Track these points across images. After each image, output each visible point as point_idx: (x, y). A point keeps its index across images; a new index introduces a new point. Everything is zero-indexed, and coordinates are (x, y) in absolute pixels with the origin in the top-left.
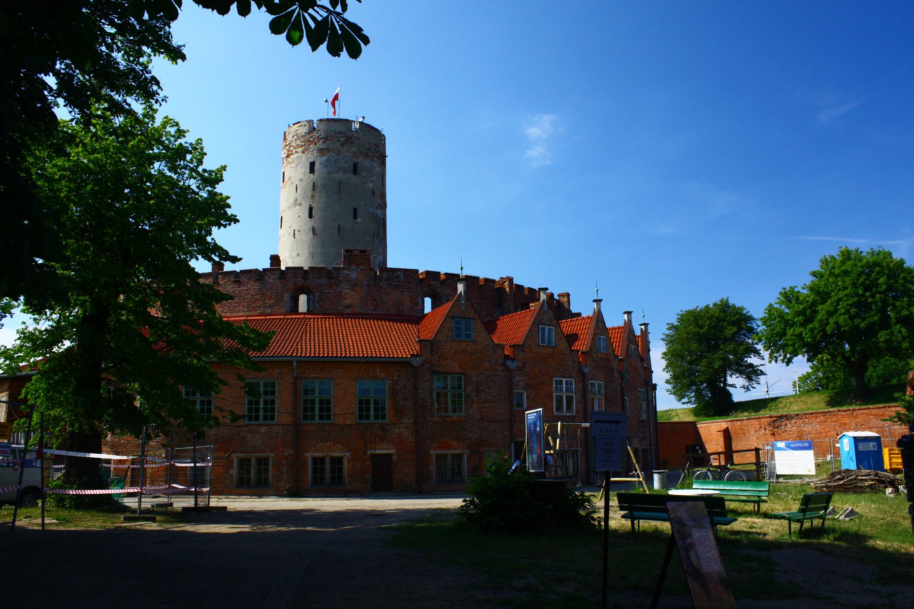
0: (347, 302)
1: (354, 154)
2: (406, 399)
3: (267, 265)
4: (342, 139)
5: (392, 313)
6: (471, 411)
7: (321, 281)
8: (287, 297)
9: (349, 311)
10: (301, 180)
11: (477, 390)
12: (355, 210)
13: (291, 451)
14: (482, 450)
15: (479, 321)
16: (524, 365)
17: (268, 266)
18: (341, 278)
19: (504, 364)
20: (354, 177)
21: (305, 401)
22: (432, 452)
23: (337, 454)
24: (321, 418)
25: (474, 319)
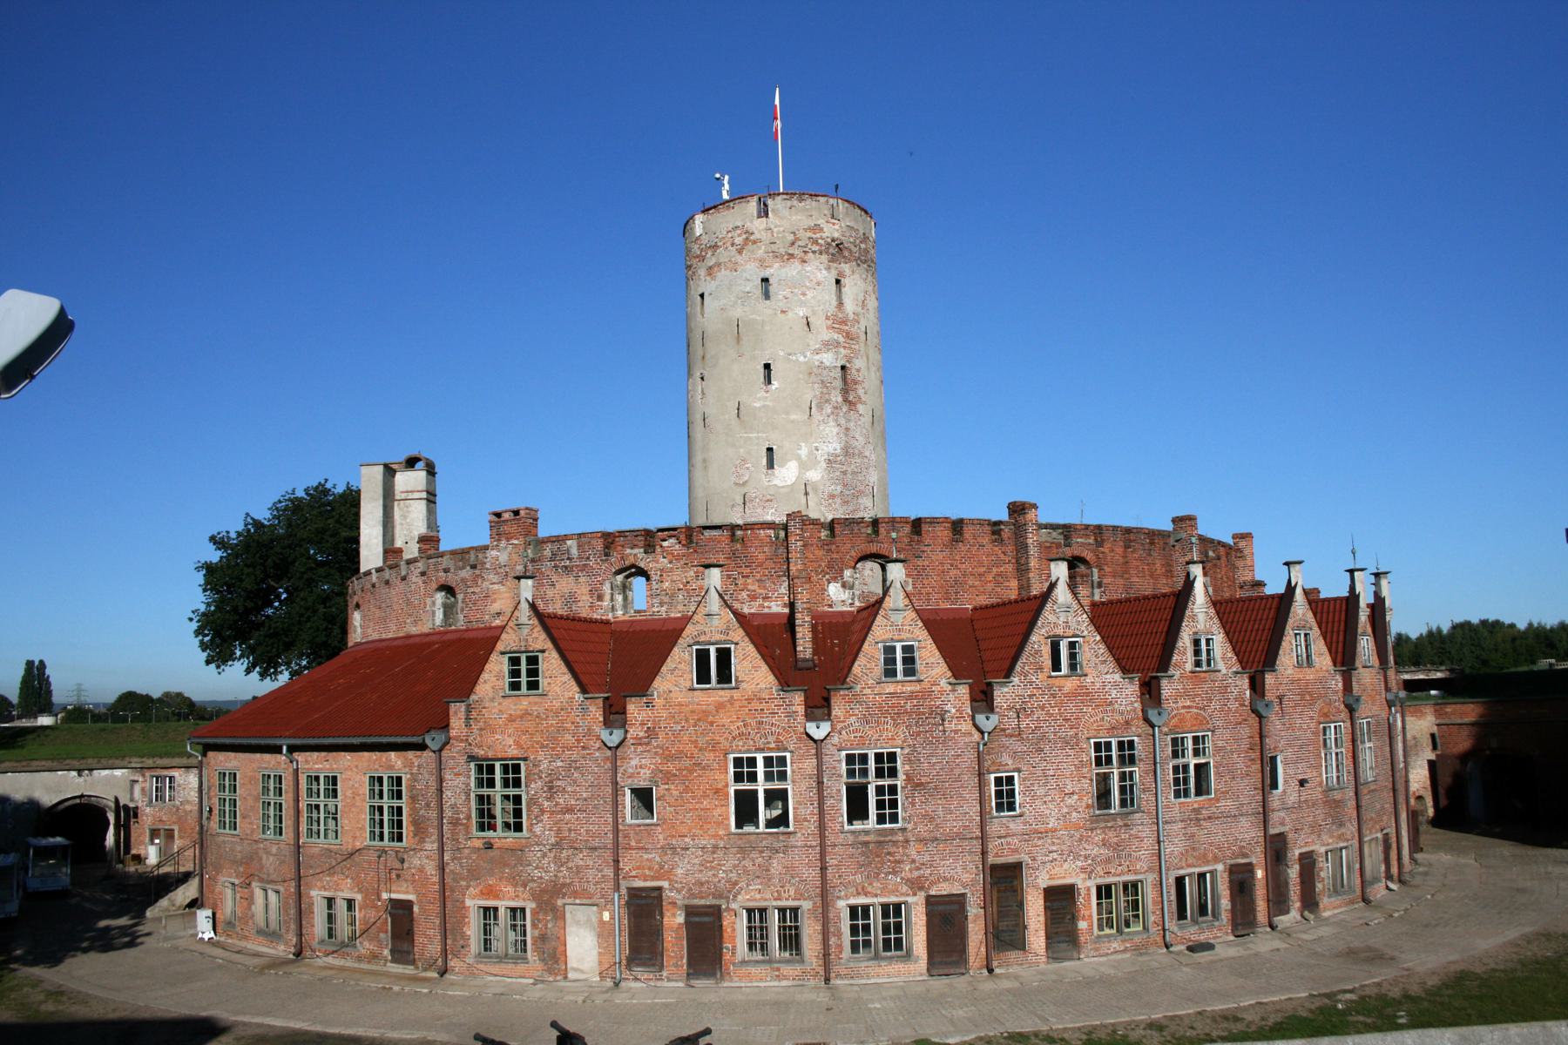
0: (496, 607)
1: (762, 261)
2: (428, 805)
4: (738, 240)
6: (538, 829)
11: (551, 788)
12: (767, 366)
14: (560, 902)
22: (469, 903)
25: (543, 651)
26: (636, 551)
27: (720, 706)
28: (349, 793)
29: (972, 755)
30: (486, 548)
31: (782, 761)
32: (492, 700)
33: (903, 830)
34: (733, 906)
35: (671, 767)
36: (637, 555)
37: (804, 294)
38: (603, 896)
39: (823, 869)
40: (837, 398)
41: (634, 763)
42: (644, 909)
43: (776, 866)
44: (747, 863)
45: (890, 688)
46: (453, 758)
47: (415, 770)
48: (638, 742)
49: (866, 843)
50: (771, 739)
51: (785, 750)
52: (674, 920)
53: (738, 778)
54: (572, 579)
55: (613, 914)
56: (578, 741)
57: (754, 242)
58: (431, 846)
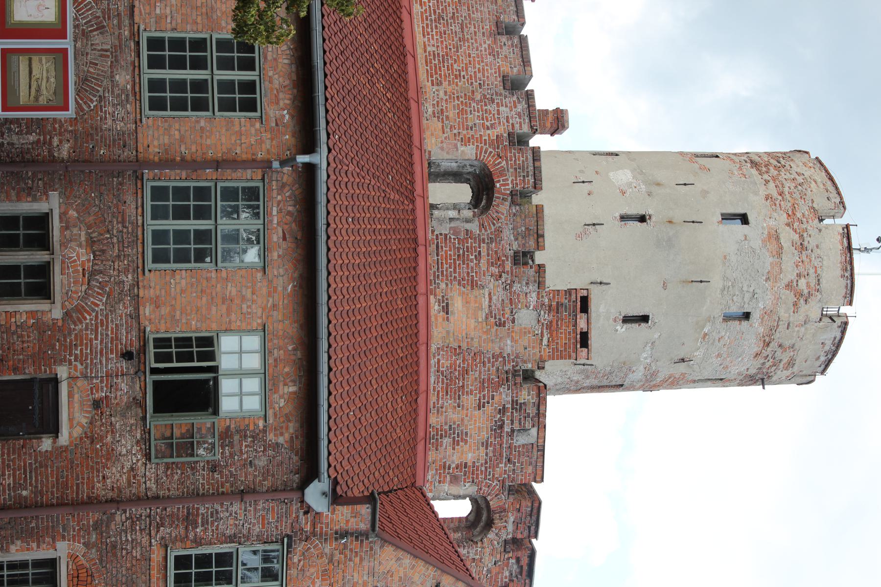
0: (457, 304)
3: (544, 102)
5: (433, 420)
7: (508, 234)
8: (469, 152)
9: (435, 307)
10: (704, 193)
12: (645, 319)
13: (65, 154)
17: (541, 103)
18: (516, 287)
20: (718, 313)
21: (202, 193)
22: (62, 550)
23: (58, 280)
24: (159, 236)
26: (510, 528)
28: (231, 290)
30: (541, 284)
32: (372, 573)
36: (506, 527)
37: (719, 355)
40: (587, 383)
46: (288, 514)
47: (271, 437)
54: (485, 435)
57: (795, 304)
58: (151, 477)
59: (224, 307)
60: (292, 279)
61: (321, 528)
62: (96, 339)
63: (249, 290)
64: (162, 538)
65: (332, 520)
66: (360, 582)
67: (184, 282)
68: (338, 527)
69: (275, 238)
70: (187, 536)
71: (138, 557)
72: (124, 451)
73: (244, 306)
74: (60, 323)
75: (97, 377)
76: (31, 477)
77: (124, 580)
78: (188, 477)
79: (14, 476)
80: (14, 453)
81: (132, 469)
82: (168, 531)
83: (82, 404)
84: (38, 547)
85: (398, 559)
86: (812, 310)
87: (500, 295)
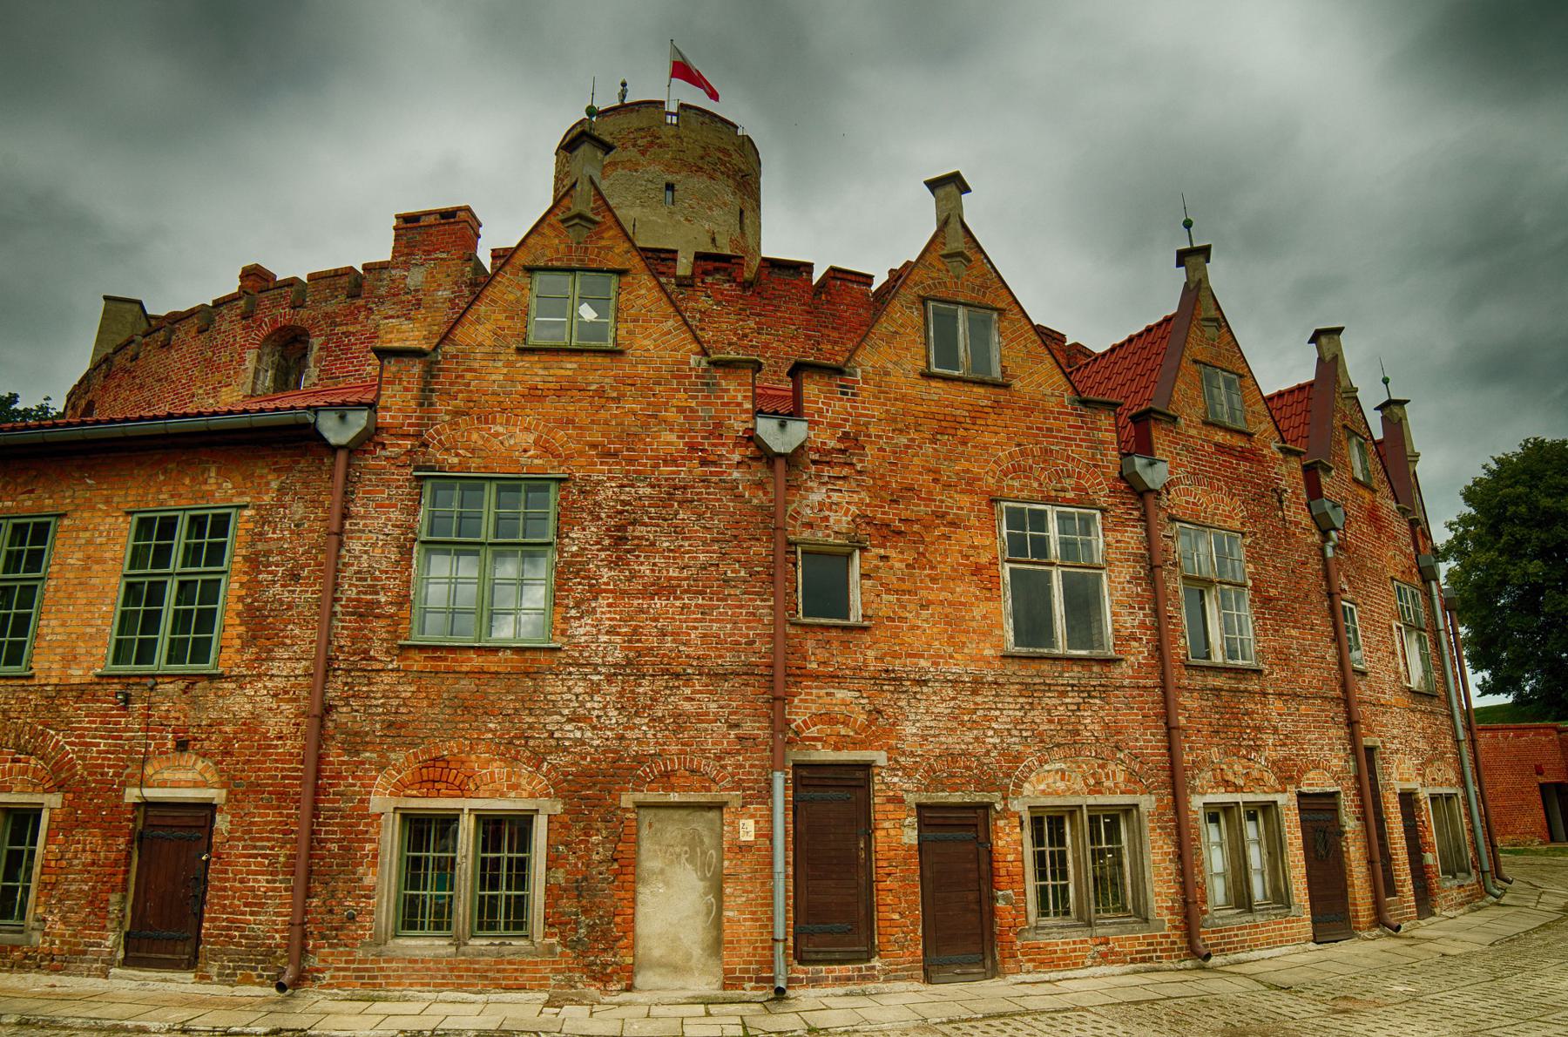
7: (330, 307)
11: (619, 541)
15: (646, 279)
16: (852, 442)
18: (383, 291)
19: (751, 438)
27: (977, 414)
29: (1315, 565)
31: (1087, 522)
32: (493, 356)
33: (1259, 672)
34: (1017, 806)
35: (891, 514)
37: (710, 209)
38: (738, 785)
39: (1170, 730)
41: (817, 497)
42: (831, 802)
43: (1091, 724)
44: (1037, 715)
45: (1220, 437)
48: (825, 458)
49: (1217, 691)
50: (1068, 483)
51: (1093, 505)
52: (897, 834)
53: (1016, 547)
55: (762, 826)
56: (692, 447)
58: (287, 667)
59: (95, 567)
60: (81, 480)
61: (410, 425)
62: (98, 745)
63: (81, 534)
64: (388, 652)
65: (400, 410)
66: (505, 371)
67: (53, 623)
68: (413, 404)
69: (29, 503)
70: (391, 616)
71: (414, 688)
72: (249, 707)
73: (98, 541)
74: (70, 796)
75: (147, 746)
76: (263, 848)
77: (448, 711)
78: (300, 614)
79: (256, 873)
80: (226, 872)
81: (275, 695)
82: (377, 643)
83: (179, 768)
84: (372, 841)
85: (478, 321)
86: (666, 134)
87: (388, 309)
